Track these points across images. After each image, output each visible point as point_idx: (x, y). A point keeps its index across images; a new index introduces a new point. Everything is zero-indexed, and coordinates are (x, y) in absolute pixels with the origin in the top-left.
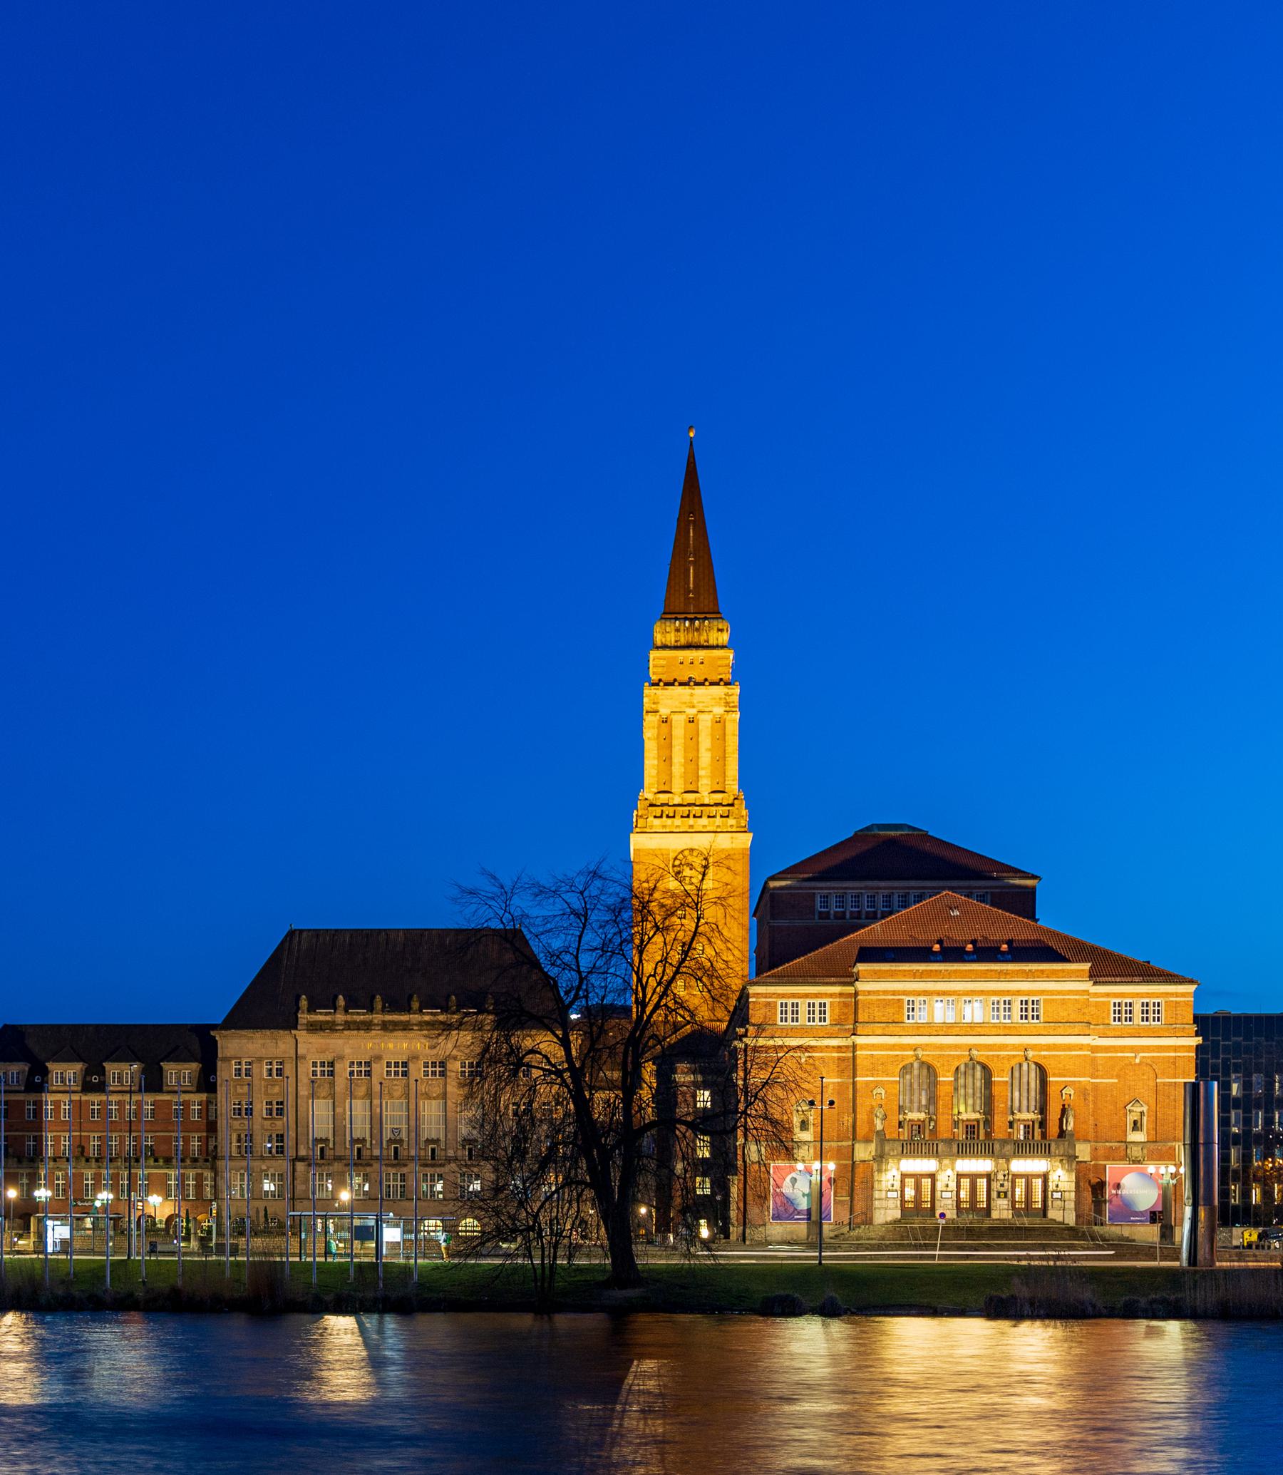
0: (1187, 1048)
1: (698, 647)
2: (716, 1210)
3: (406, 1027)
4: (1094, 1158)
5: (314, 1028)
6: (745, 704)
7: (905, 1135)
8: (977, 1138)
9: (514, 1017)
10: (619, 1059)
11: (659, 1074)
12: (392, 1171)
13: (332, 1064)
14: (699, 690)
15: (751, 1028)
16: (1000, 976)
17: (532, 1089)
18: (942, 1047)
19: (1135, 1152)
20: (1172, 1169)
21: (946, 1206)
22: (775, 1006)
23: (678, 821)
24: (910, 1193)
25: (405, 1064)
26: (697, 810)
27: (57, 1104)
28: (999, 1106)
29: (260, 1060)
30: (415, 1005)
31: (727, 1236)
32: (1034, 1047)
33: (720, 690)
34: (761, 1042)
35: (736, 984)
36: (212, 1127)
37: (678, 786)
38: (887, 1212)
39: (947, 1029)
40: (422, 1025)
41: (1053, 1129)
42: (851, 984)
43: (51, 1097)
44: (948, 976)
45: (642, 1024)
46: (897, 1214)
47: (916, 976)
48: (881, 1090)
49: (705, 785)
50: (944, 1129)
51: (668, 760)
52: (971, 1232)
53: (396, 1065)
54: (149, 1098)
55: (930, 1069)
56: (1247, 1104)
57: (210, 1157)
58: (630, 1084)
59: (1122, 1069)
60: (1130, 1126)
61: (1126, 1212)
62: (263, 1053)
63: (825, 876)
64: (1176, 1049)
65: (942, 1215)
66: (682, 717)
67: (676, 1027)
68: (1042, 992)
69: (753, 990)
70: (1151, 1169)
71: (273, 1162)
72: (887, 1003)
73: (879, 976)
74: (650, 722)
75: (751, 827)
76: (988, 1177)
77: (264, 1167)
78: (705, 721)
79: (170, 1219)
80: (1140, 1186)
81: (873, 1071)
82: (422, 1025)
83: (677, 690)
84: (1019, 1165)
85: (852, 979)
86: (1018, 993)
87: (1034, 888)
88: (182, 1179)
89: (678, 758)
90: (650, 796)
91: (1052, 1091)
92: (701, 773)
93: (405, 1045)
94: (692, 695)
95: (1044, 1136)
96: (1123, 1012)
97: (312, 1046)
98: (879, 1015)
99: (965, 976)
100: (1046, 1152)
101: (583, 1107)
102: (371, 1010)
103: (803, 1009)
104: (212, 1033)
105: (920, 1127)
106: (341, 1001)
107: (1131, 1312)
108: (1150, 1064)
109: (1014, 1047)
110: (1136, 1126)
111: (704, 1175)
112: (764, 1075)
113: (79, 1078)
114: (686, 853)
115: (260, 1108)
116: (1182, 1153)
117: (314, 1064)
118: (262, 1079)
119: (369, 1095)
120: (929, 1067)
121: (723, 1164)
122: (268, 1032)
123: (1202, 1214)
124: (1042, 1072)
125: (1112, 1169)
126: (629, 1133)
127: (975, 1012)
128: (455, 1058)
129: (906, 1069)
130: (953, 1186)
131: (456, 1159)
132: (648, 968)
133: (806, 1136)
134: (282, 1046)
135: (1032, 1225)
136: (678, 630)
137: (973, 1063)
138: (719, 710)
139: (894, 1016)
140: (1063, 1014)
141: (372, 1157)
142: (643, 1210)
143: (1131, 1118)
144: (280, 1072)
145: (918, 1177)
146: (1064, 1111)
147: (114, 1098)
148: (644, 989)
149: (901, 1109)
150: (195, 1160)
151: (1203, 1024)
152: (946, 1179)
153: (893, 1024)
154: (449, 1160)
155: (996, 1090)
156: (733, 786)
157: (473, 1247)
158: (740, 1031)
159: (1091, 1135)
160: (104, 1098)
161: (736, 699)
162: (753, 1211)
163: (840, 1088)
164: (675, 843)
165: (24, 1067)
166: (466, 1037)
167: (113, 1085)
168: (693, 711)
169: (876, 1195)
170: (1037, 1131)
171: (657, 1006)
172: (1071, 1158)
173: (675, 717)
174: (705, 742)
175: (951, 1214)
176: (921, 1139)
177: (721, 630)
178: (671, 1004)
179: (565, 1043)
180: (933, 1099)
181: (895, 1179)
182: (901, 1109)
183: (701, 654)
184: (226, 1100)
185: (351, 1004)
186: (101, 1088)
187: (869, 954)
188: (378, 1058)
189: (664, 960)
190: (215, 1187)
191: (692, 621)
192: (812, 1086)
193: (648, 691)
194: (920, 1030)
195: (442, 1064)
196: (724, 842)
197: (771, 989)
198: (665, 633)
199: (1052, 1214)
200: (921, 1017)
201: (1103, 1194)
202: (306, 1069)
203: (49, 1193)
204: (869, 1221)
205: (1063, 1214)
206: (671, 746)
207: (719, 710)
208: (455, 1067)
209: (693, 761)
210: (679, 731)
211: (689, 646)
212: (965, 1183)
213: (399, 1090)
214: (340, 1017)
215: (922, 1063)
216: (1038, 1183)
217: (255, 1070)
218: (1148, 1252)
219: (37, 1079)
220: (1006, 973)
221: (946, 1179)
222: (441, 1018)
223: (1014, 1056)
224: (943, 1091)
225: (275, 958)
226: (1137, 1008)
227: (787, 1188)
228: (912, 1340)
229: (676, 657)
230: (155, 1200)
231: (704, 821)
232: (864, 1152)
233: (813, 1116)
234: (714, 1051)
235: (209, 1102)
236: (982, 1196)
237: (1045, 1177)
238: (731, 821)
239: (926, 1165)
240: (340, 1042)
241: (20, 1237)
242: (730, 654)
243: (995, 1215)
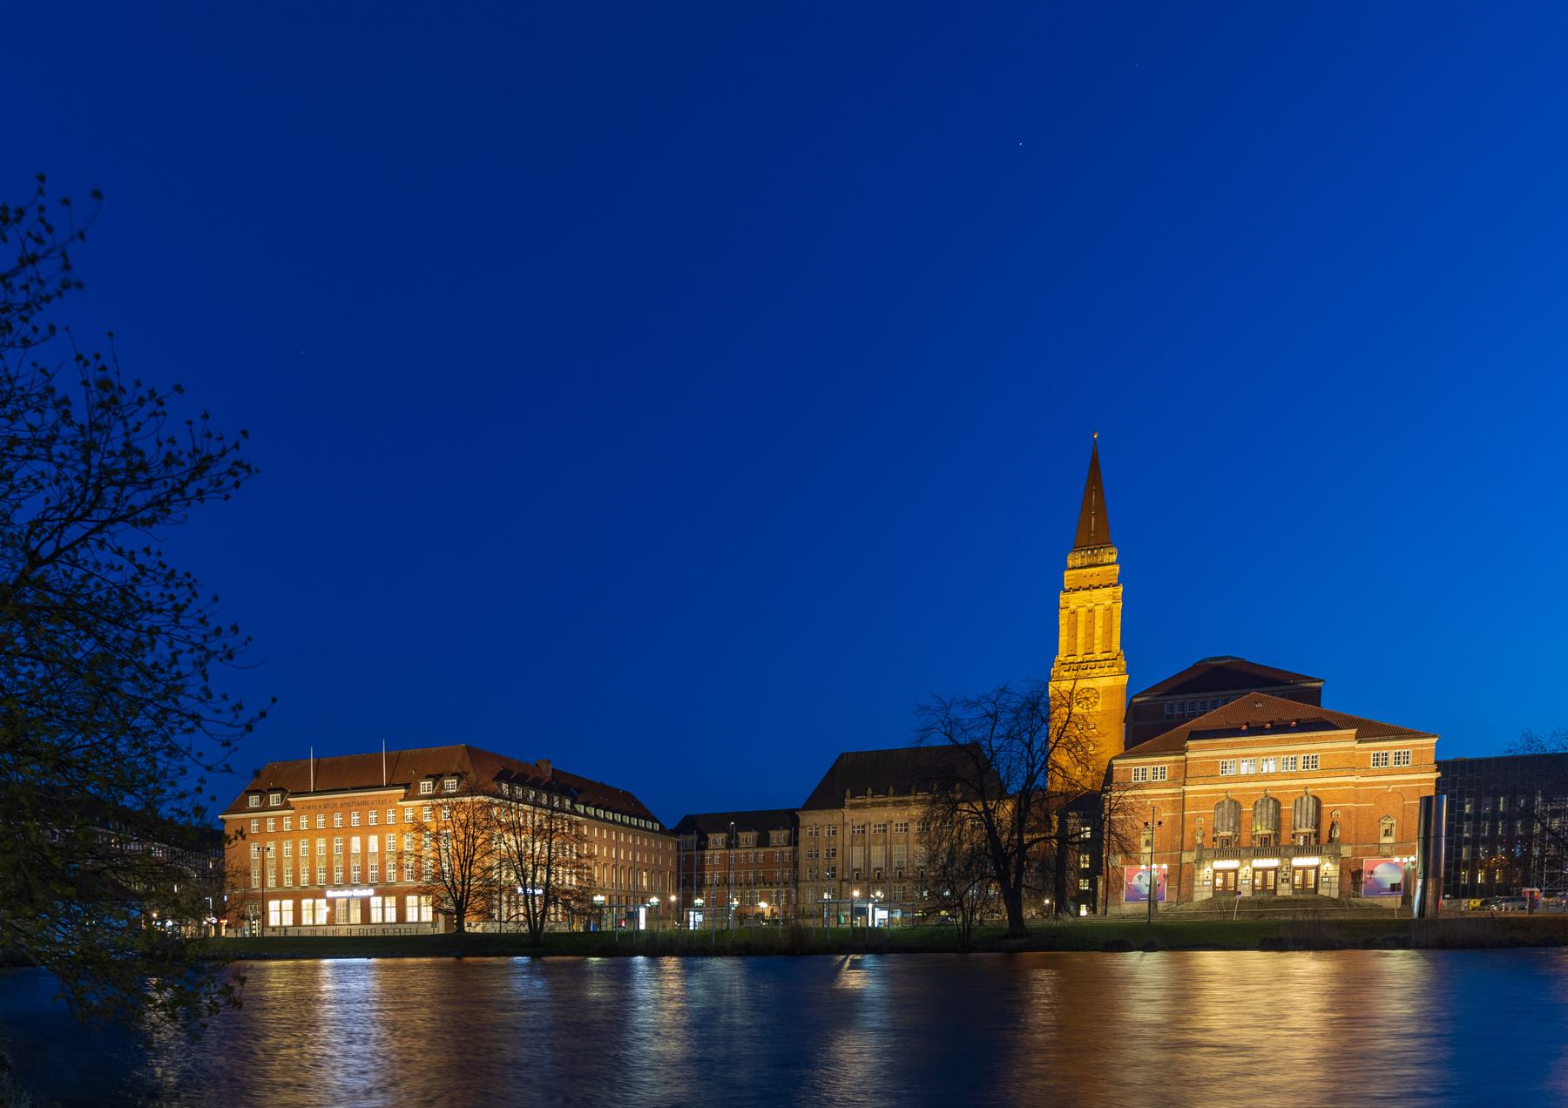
0: (1430, 780)
5: (854, 807)
7: (1217, 845)
8: (1268, 846)
16: (1289, 742)
18: (1245, 789)
19: (1386, 850)
24: (1219, 882)
28: (1285, 824)
33: (1111, 590)
35: (1106, 757)
36: (796, 865)
37: (1080, 651)
38: (1203, 893)
39: (1249, 778)
41: (1324, 837)
44: (1252, 745)
46: (1210, 895)
47: (1228, 746)
48: (1201, 819)
49: (1098, 648)
50: (1245, 840)
51: (1075, 636)
52: (1260, 903)
54: (762, 851)
55: (1236, 804)
56: (1476, 818)
57: (795, 881)
61: (1377, 889)
63: (1169, 693)
64: (1420, 781)
70: (1397, 859)
73: (1202, 748)
74: (1063, 613)
75: (1127, 672)
76: (1276, 870)
78: (1099, 610)
80: (1386, 872)
81: (1196, 807)
83: (1082, 593)
84: (1297, 862)
85: (1182, 750)
87: (1319, 689)
91: (1325, 813)
95: (1317, 842)
96: (1381, 759)
97: (849, 814)
98: (1201, 772)
99: (1263, 744)
100: (1319, 853)
102: (887, 795)
105: (1228, 840)
106: (870, 791)
107: (1369, 945)
108: (1400, 793)
109: (1298, 787)
110: (1387, 833)
115: (823, 853)
116: (1417, 846)
119: (885, 843)
123: (1431, 884)
124: (1318, 802)
125: (1366, 862)
127: (1270, 767)
129: (1220, 805)
135: (1308, 897)
137: (1267, 798)
138: (1108, 602)
139: (1211, 773)
143: (1383, 828)
145: (1225, 872)
146: (1333, 825)
149: (1215, 830)
151: (1441, 765)
152: (1245, 871)
153: (1211, 777)
155: (1283, 815)
156: (1116, 647)
163: (1173, 821)
165: (695, 837)
167: (743, 844)
170: (1313, 840)
172: (1336, 856)
174: (1099, 622)
176: (1228, 848)
180: (1238, 823)
181: (1209, 874)
182: (1215, 830)
184: (804, 849)
185: (876, 792)
187: (1195, 735)
193: (1063, 596)
194: (1229, 780)
198: (1074, 559)
199: (1320, 892)
200: (1231, 772)
202: (848, 830)
204: (1191, 900)
205: (1330, 891)
207: (1108, 602)
209: (1090, 636)
210: (1082, 619)
211: (1090, 566)
212: (1259, 874)
213: (902, 839)
214: (869, 800)
215: (1231, 801)
221: (1245, 871)
224: (1245, 817)
225: (833, 769)
226: (1391, 756)
227: (1135, 881)
230: (763, 905)
232: (1187, 858)
234: (1091, 805)
236: (1271, 881)
237: (1317, 869)
239: (1232, 864)
242: (1117, 568)
243: (1279, 893)
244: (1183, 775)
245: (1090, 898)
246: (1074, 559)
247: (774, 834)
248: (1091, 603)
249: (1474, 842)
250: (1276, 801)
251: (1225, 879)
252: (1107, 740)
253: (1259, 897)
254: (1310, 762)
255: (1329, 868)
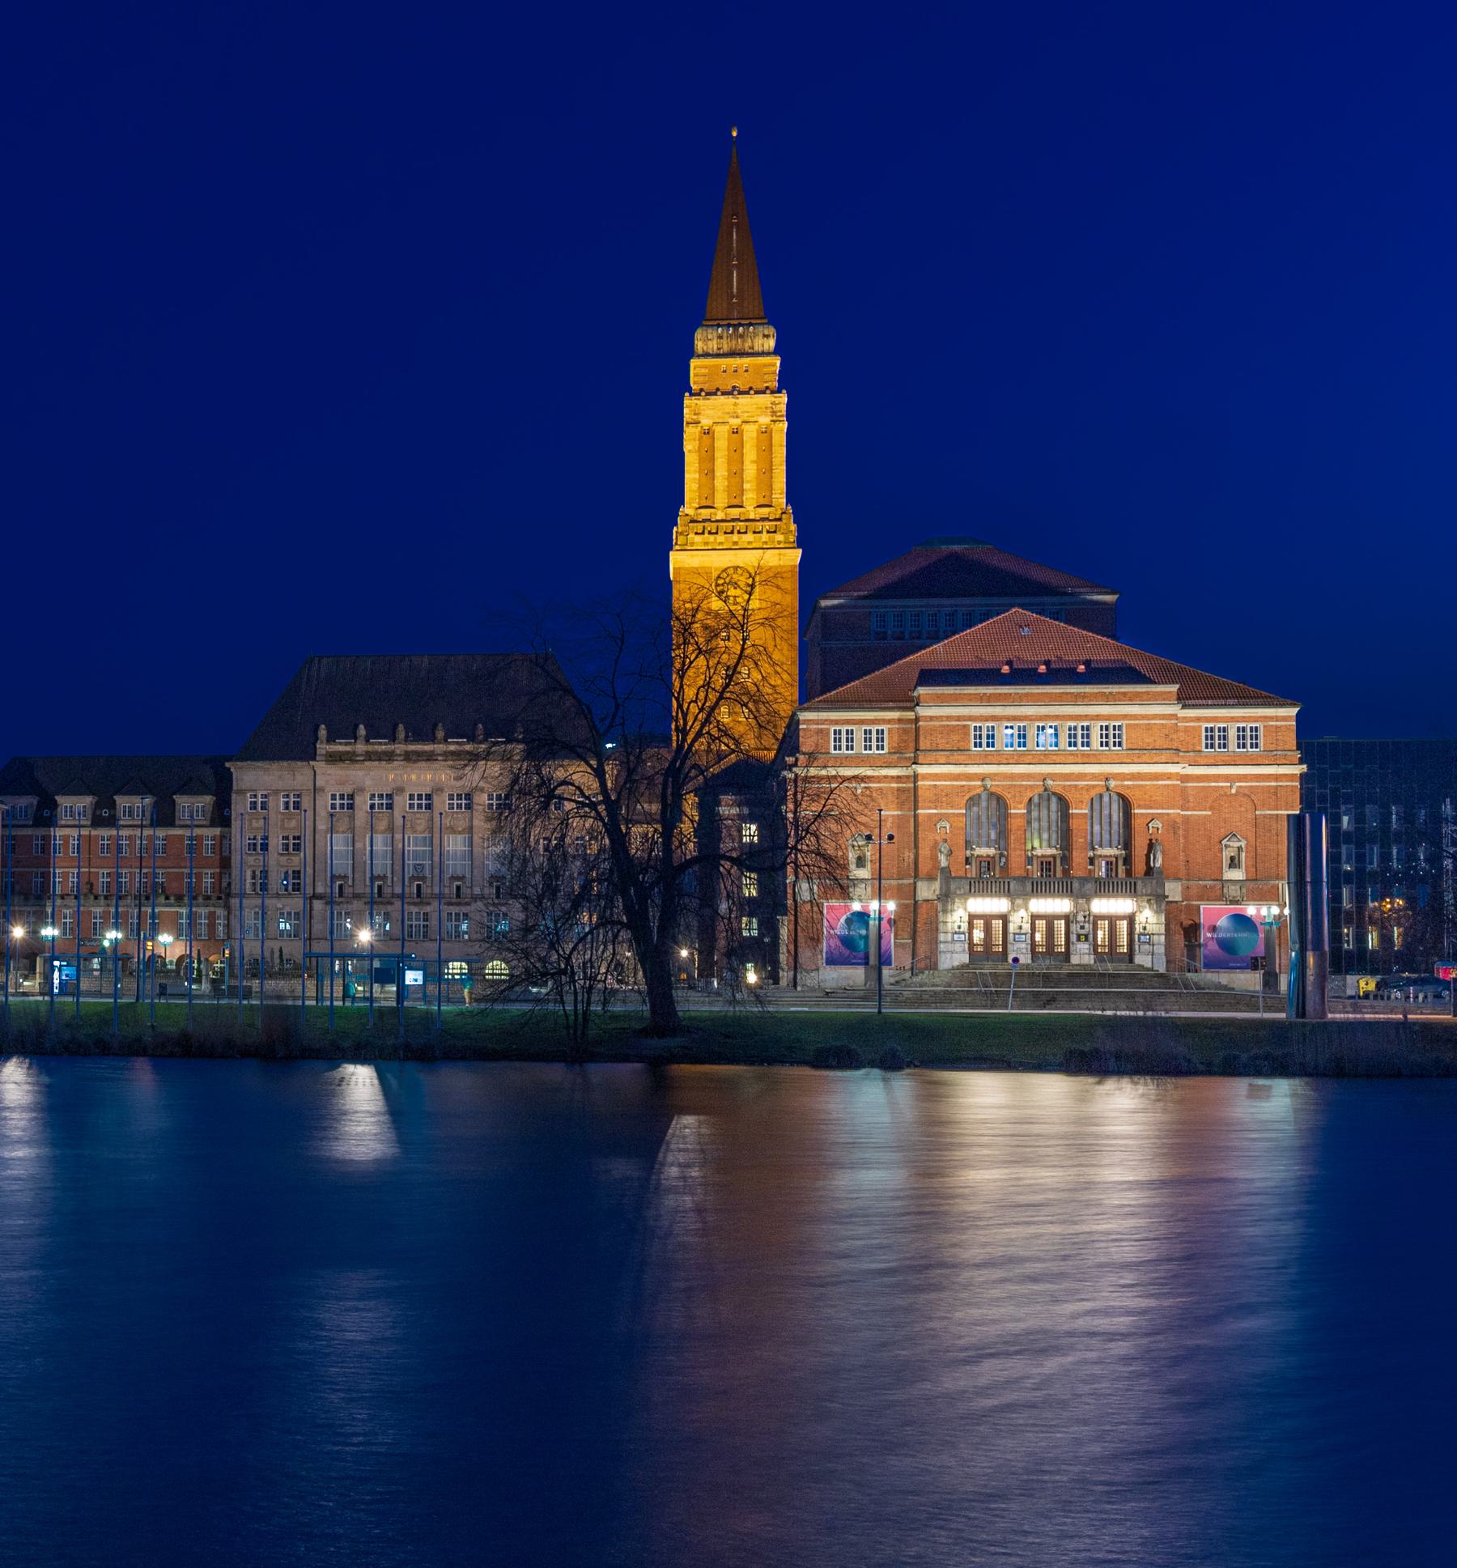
1: (742, 354)
2: (765, 953)
3: (430, 757)
4: (1186, 898)
5: (334, 758)
6: (793, 413)
7: (973, 871)
8: (1054, 875)
9: (546, 746)
10: (659, 789)
11: (701, 807)
12: (414, 909)
13: (351, 797)
14: (743, 400)
15: (801, 757)
16: (1076, 699)
17: (565, 822)
18: (1012, 777)
19: (1233, 891)
20: (1275, 910)
21: (1020, 951)
22: (828, 734)
23: (721, 538)
24: (978, 935)
25: (429, 797)
26: (741, 526)
27: (66, 838)
28: (1078, 841)
29: (276, 792)
30: (440, 734)
31: (776, 981)
32: (1116, 776)
33: (766, 399)
34: (813, 772)
35: (785, 709)
36: (225, 863)
37: (721, 500)
38: (952, 956)
40: (447, 755)
41: (1139, 866)
42: (912, 709)
43: (59, 832)
44: (1019, 700)
45: (683, 754)
46: (965, 959)
48: (944, 822)
49: (750, 498)
51: (711, 474)
52: (1047, 978)
53: (420, 797)
54: (161, 833)
55: (999, 801)
57: (224, 894)
58: (670, 817)
59: (1217, 799)
60: (1226, 862)
62: (280, 785)
65: (1016, 960)
66: (726, 428)
67: (720, 756)
68: (1125, 717)
69: (804, 716)
71: (289, 901)
72: (953, 729)
73: (941, 701)
75: (800, 543)
76: (1067, 919)
77: (280, 906)
78: (750, 432)
79: (180, 959)
81: (936, 802)
82: (447, 755)
84: (1101, 906)
85: (913, 703)
86: (1098, 717)
88: (191, 916)
89: (721, 471)
90: (687, 511)
91: (1138, 824)
92: (746, 486)
93: (429, 777)
94: (735, 404)
95: (1129, 873)
97: (331, 778)
98: (942, 742)
100: (1132, 891)
101: (619, 841)
103: (859, 736)
104: (227, 765)
105: (989, 863)
106: (362, 730)
109: (1094, 777)
110: (1234, 863)
111: (750, 915)
112: (816, 807)
113: (89, 813)
114: (731, 571)
115: (276, 843)
116: (1285, 890)
117: (333, 797)
118: (278, 812)
119: (391, 829)
120: (999, 799)
121: (771, 906)
122: (285, 764)
124: (1126, 804)
126: (669, 871)
128: (482, 790)
129: (973, 801)
130: (1027, 927)
131: (482, 897)
132: (690, 693)
133: (863, 873)
134: (299, 777)
135: (1116, 969)
136: (720, 337)
137: (1048, 794)
138: (765, 420)
140: (1149, 740)
141: (393, 895)
142: (684, 953)
143: (1226, 854)
144: (297, 806)
145: (987, 919)
146: (1151, 846)
147: (124, 833)
148: (685, 716)
149: (968, 844)
150: (208, 898)
153: (957, 752)
154: (475, 898)
155: (1074, 824)
156: (780, 497)
157: (503, 991)
158: (790, 760)
159: (1182, 873)
160: (114, 832)
161: (783, 408)
162: (805, 955)
163: (900, 821)
164: (719, 561)
166: (494, 768)
168: (738, 421)
169: (942, 937)
170: (1121, 868)
171: (699, 734)
172: (1158, 898)
173: (718, 429)
174: (750, 454)
175: (1025, 959)
176: (991, 876)
177: (767, 336)
178: (715, 732)
179: (599, 773)
182: (968, 844)
183: (746, 361)
186: (111, 822)
187: (930, 677)
188: (401, 790)
189: (707, 685)
190: (228, 926)
191: (736, 327)
192: (868, 818)
193: (688, 402)
195: (468, 796)
196: (772, 559)
197: (824, 715)
199: (1139, 959)
201: (1197, 937)
202: (324, 802)
203: (56, 932)
204: (933, 966)
206: (712, 459)
207: (765, 420)
208: (482, 799)
209: (736, 474)
210: (721, 444)
211: (732, 354)
212: (1041, 924)
213: (422, 824)
215: (991, 794)
216: (1123, 925)
217: (271, 804)
218: (1246, 1000)
219: (46, 813)
220: (1084, 696)
222: (468, 747)
223: (1094, 787)
224: (1015, 824)
228: (983, 1096)
229: (717, 366)
230: (165, 938)
231: (750, 537)
232: (927, 891)
233: (870, 852)
234: (760, 783)
235: (222, 837)
236: (1060, 939)
237: (1131, 919)
238: (779, 537)
239: (996, 905)
240: (360, 773)
241: (26, 978)
243: (1075, 960)
244: (912, 745)
245: (765, 953)
246: (705, 339)
247: (183, 801)
248: (735, 421)
249: (1360, 879)
250: (1061, 799)
251: (988, 929)
252: (776, 667)
253: (1044, 966)
254: (1112, 736)
255: (1149, 919)
